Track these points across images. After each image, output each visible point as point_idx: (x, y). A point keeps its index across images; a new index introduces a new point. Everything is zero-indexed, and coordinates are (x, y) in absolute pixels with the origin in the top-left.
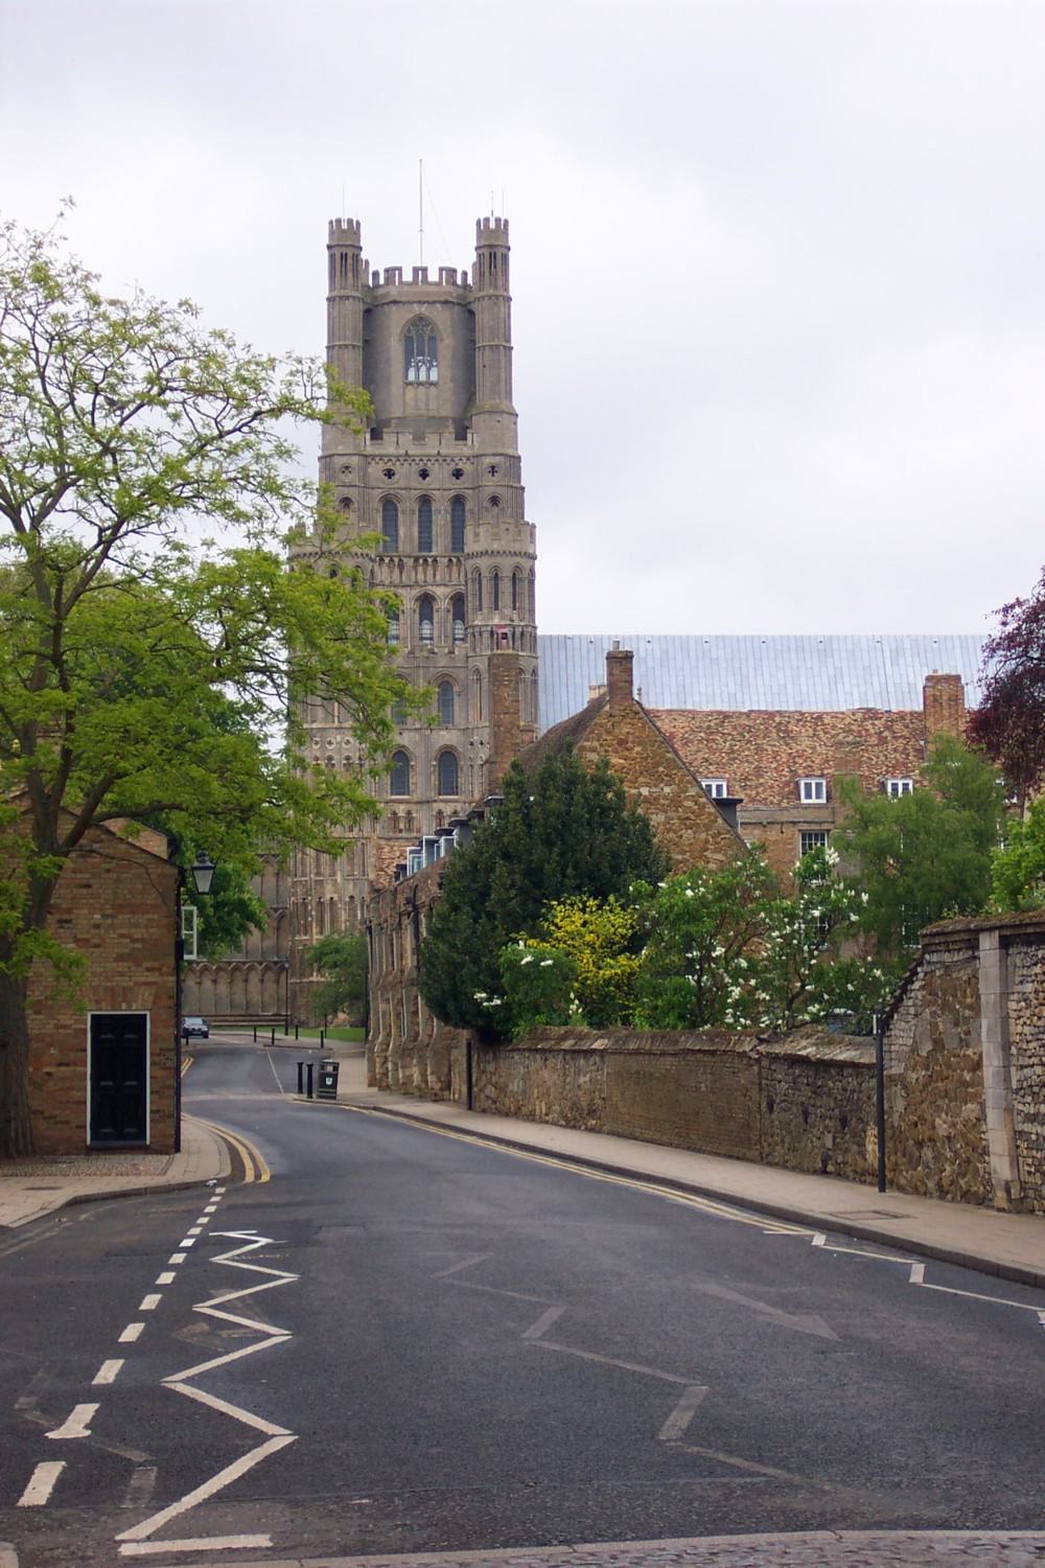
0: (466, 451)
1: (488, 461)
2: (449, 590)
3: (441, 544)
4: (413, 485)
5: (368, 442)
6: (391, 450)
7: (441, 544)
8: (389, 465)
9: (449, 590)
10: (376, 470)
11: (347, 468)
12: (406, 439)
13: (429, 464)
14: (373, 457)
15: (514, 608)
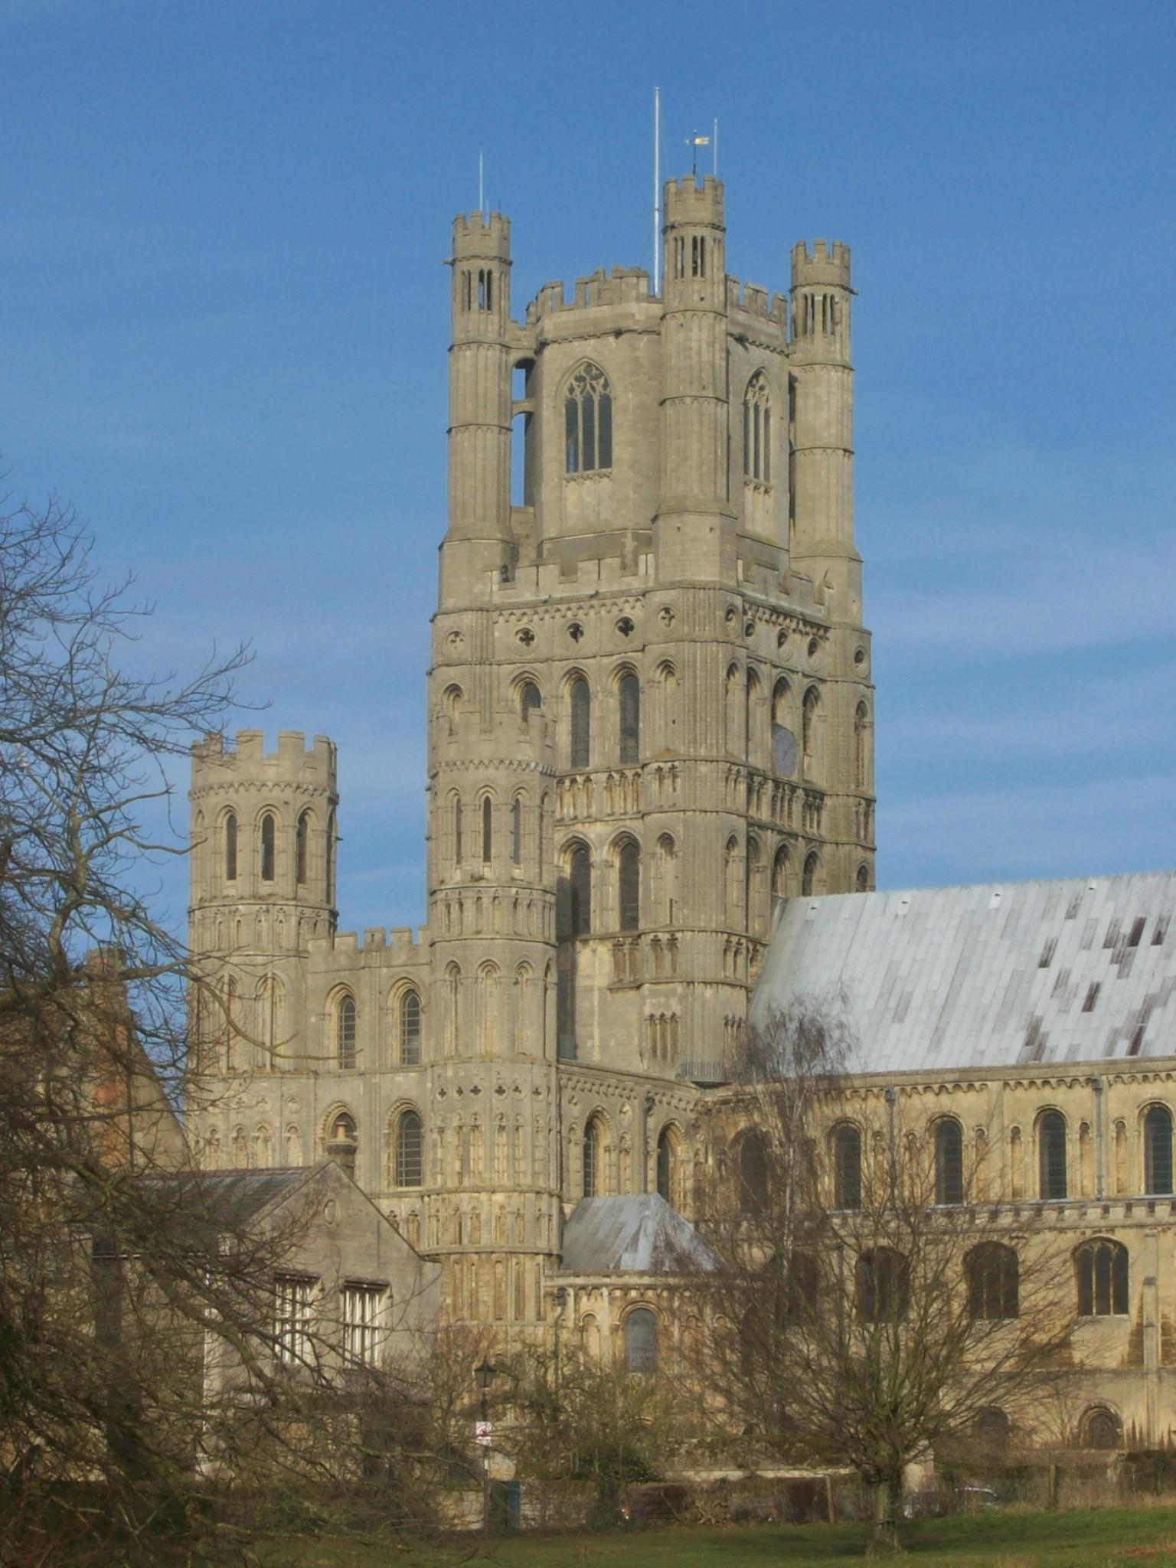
0: (635, 584)
1: (660, 598)
2: (609, 829)
3: (604, 747)
4: (558, 651)
5: (495, 587)
6: (528, 597)
7: (604, 747)
8: (524, 623)
9: (609, 829)
10: (504, 633)
11: (457, 634)
12: (550, 573)
13: (581, 612)
14: (500, 609)
15: (487, 857)
